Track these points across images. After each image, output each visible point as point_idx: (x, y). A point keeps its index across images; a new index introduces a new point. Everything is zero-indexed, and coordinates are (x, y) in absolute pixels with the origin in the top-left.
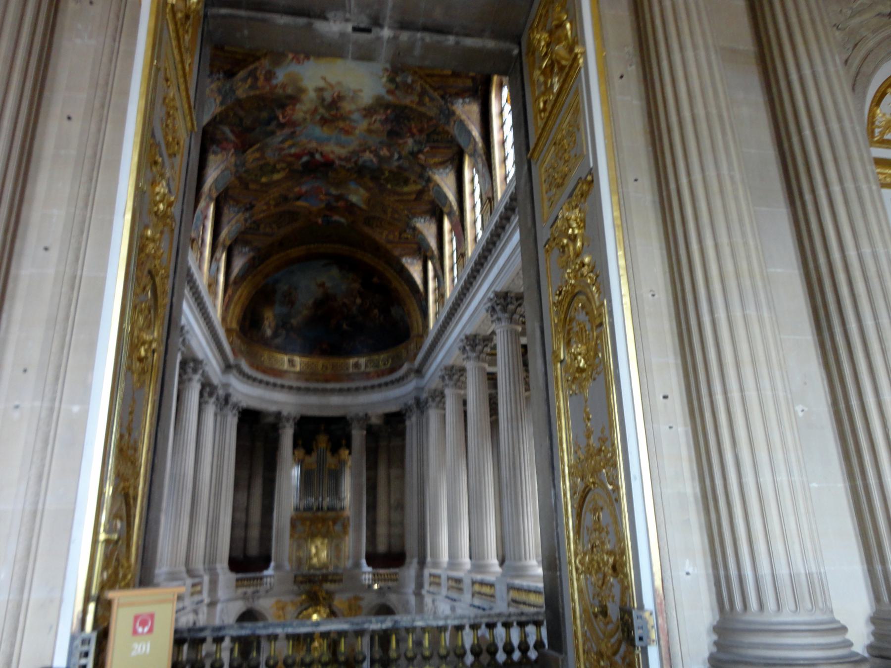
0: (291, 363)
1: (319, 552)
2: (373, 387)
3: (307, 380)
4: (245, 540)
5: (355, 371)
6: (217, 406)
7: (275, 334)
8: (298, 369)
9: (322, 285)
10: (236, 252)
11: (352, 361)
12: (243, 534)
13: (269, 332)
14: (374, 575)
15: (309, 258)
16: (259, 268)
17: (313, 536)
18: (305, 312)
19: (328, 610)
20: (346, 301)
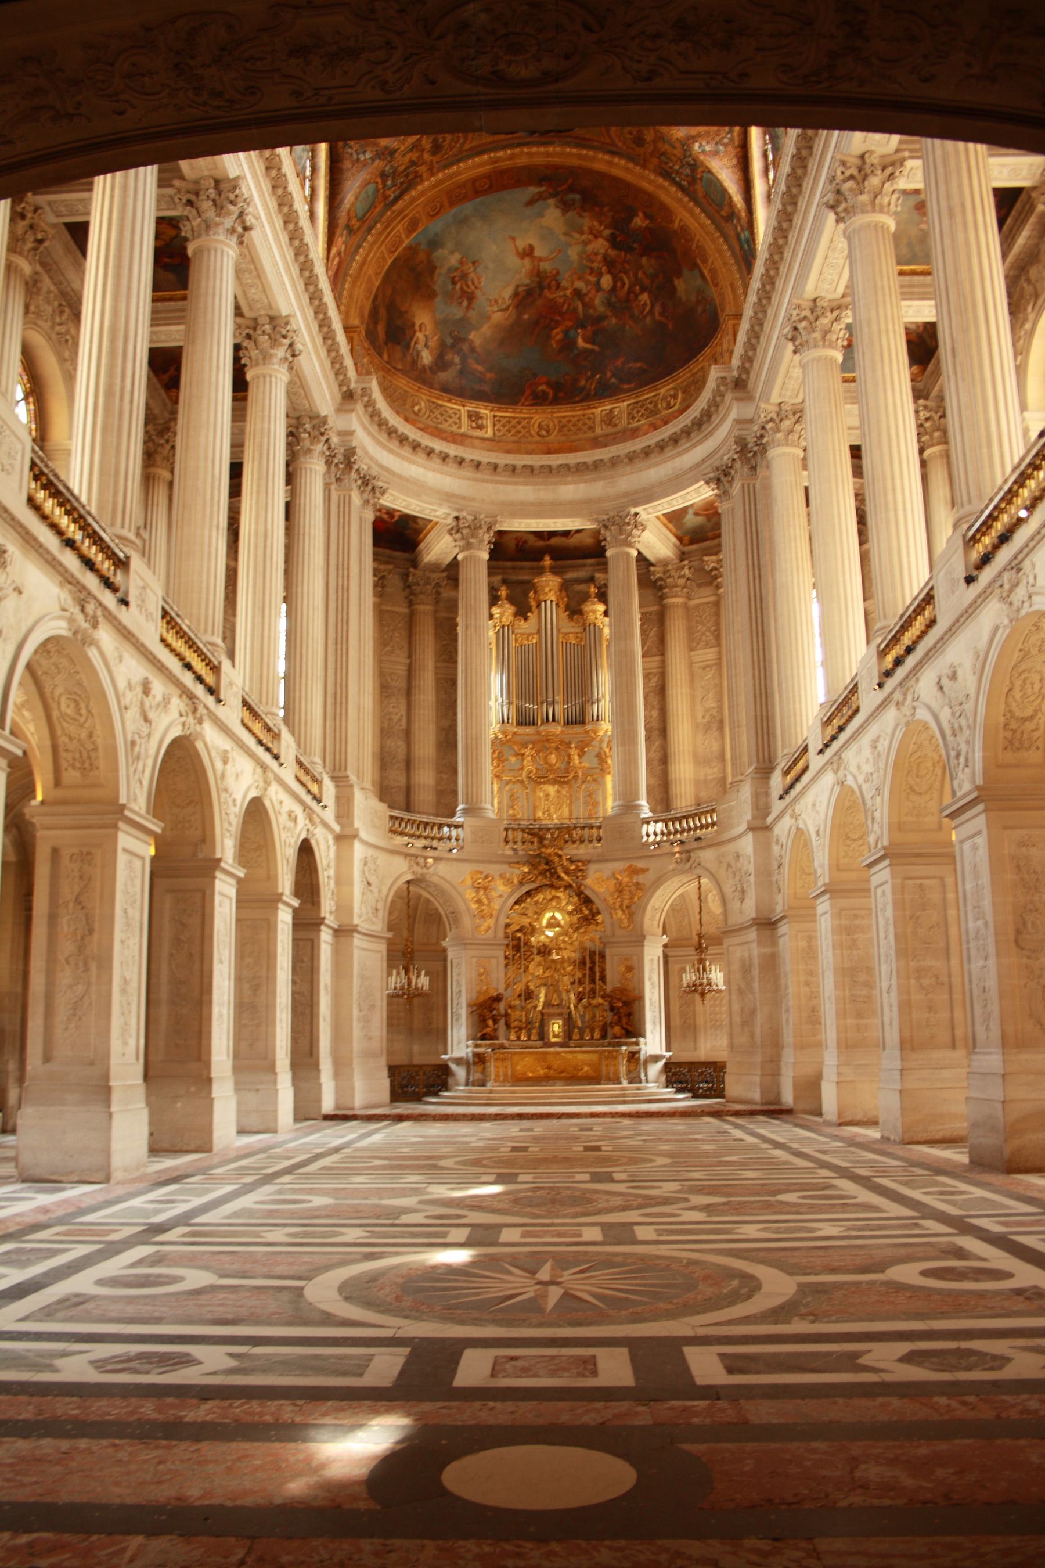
0: (474, 417)
1: (552, 807)
2: (647, 452)
3: (508, 452)
4: (409, 790)
5: (610, 430)
6: (328, 471)
7: (441, 363)
8: (490, 433)
9: (528, 253)
10: (347, 164)
11: (601, 410)
12: (402, 780)
13: (426, 358)
14: (665, 822)
15: (499, 182)
16: (396, 207)
17: (539, 779)
18: (498, 317)
19: (576, 899)
20: (580, 285)
